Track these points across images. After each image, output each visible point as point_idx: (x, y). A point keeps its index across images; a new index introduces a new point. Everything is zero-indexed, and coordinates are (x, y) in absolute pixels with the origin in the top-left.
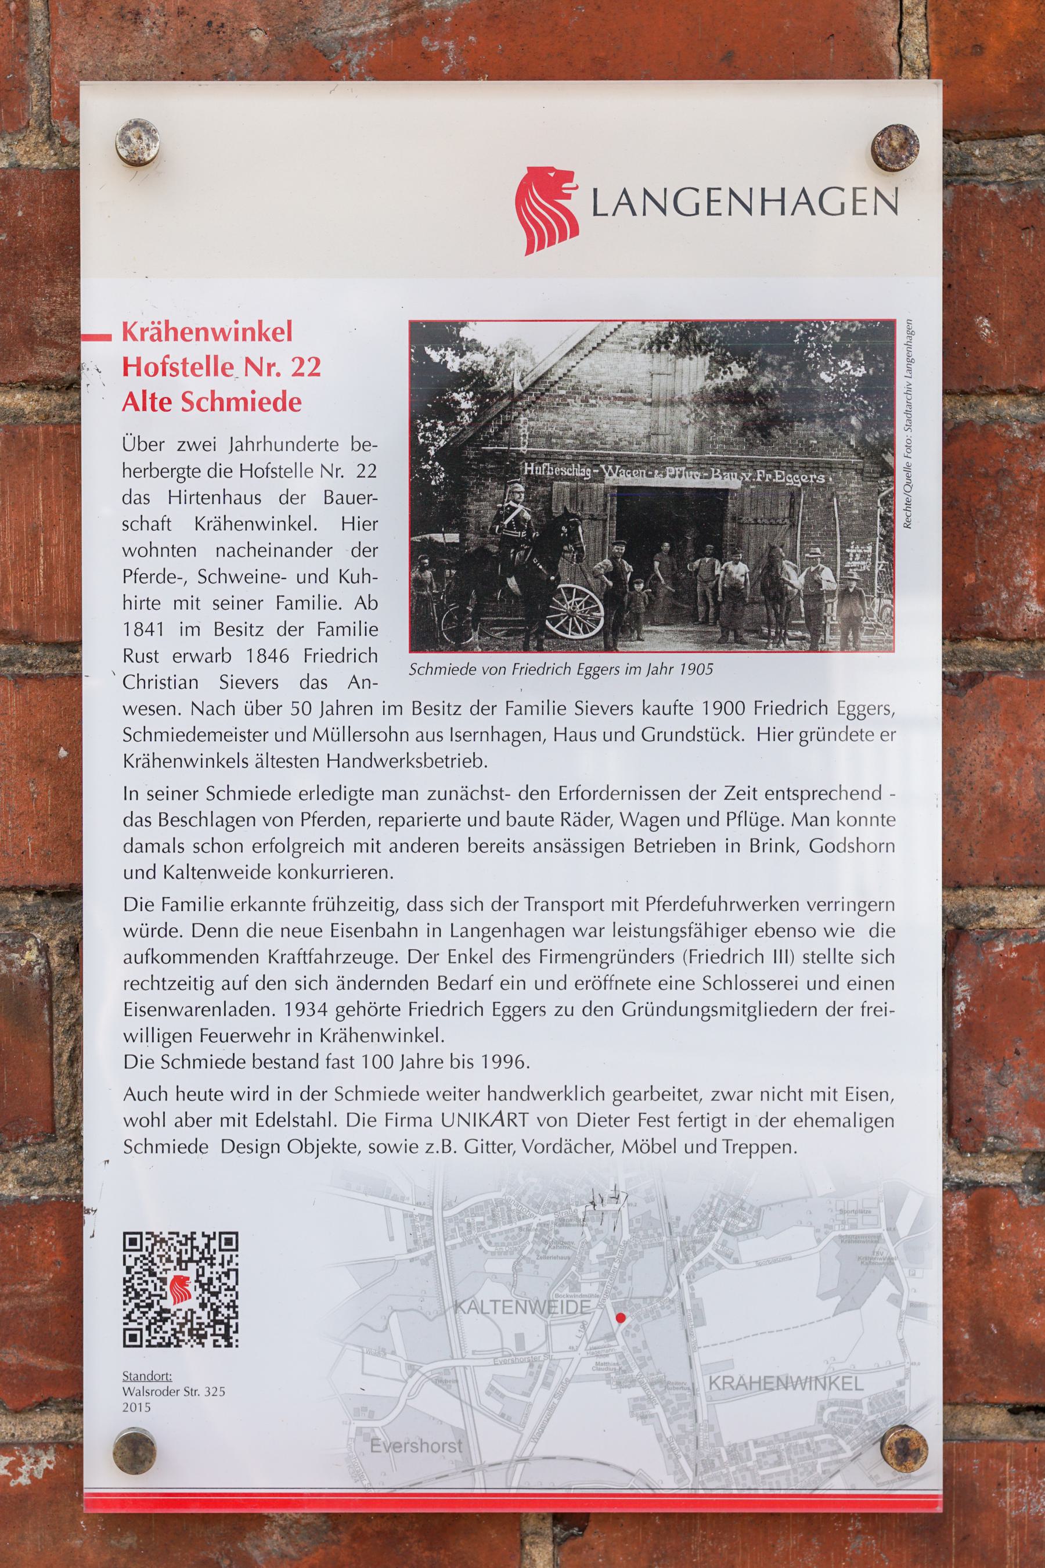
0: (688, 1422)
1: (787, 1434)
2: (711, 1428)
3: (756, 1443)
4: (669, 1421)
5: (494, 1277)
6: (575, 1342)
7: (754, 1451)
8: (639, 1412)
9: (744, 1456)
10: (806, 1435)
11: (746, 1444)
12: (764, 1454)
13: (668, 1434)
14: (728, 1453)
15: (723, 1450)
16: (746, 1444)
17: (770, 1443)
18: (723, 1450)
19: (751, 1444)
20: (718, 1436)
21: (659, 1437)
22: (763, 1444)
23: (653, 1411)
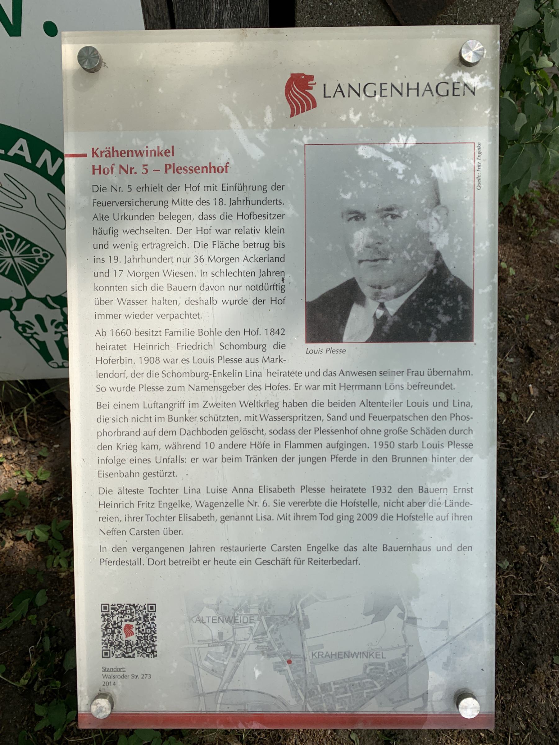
0: (302, 674)
1: (349, 678)
2: (313, 676)
3: (334, 684)
4: (292, 672)
5: (208, 606)
6: (248, 636)
7: (333, 687)
8: (278, 669)
9: (329, 689)
10: (358, 679)
11: (330, 683)
12: (338, 688)
13: (292, 679)
14: (321, 688)
15: (318, 686)
16: (330, 683)
17: (341, 683)
18: (318, 686)
19: (332, 683)
20: (316, 680)
21: (288, 680)
22: (338, 684)
23: (284, 668)
